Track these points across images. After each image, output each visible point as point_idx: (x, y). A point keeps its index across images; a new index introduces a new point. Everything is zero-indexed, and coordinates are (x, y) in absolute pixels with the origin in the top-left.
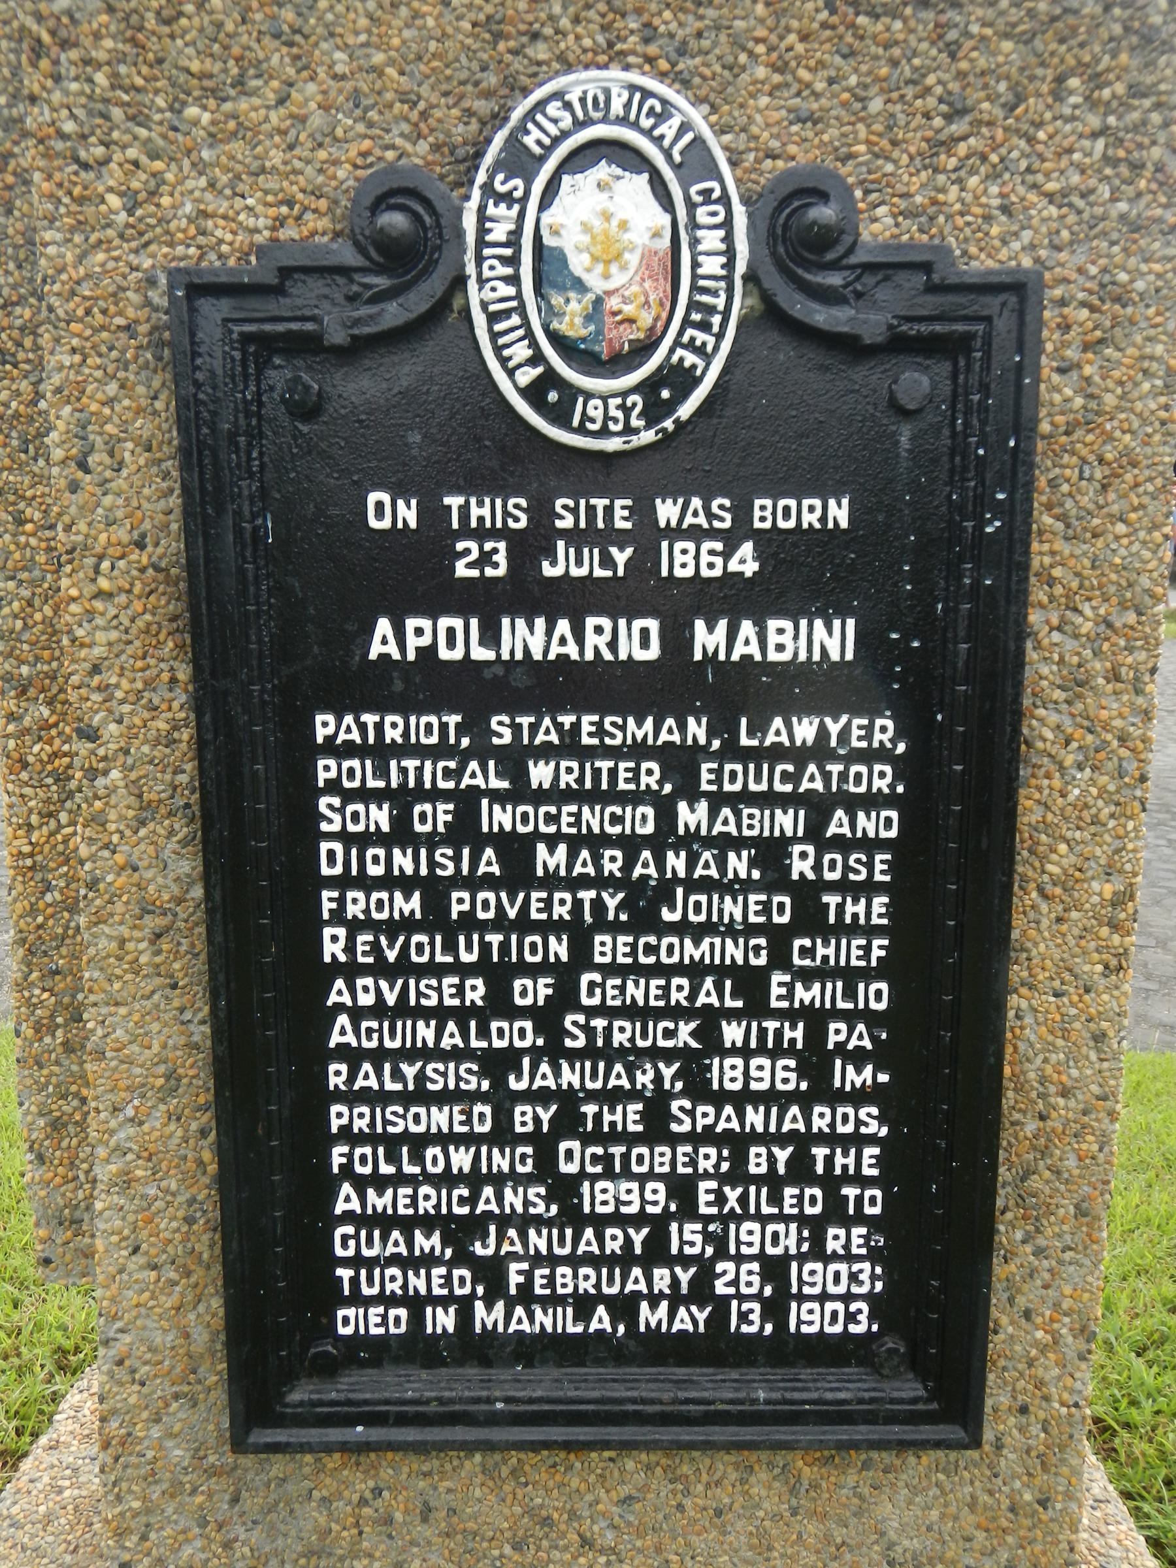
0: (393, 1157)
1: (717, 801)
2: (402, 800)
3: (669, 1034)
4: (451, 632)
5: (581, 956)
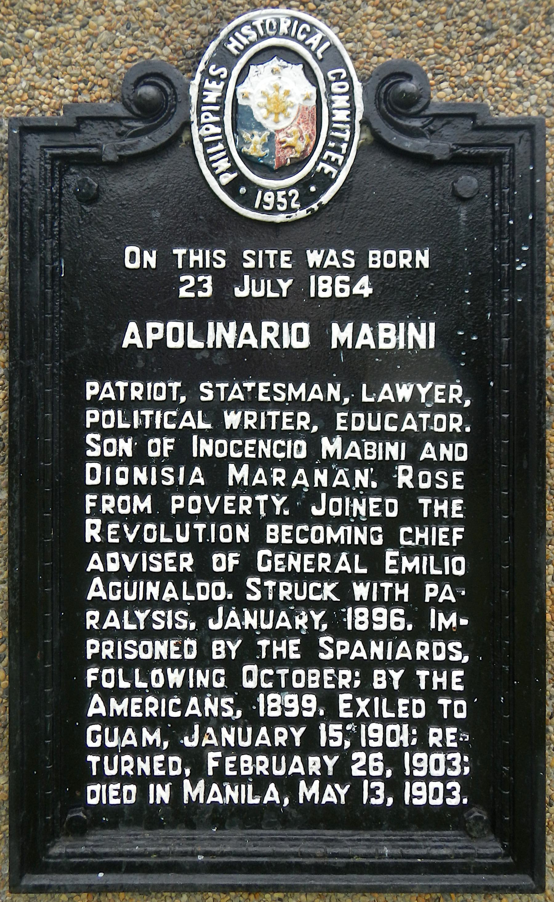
0: (128, 677)
1: (348, 437)
2: (141, 436)
3: (317, 591)
5: (258, 538)
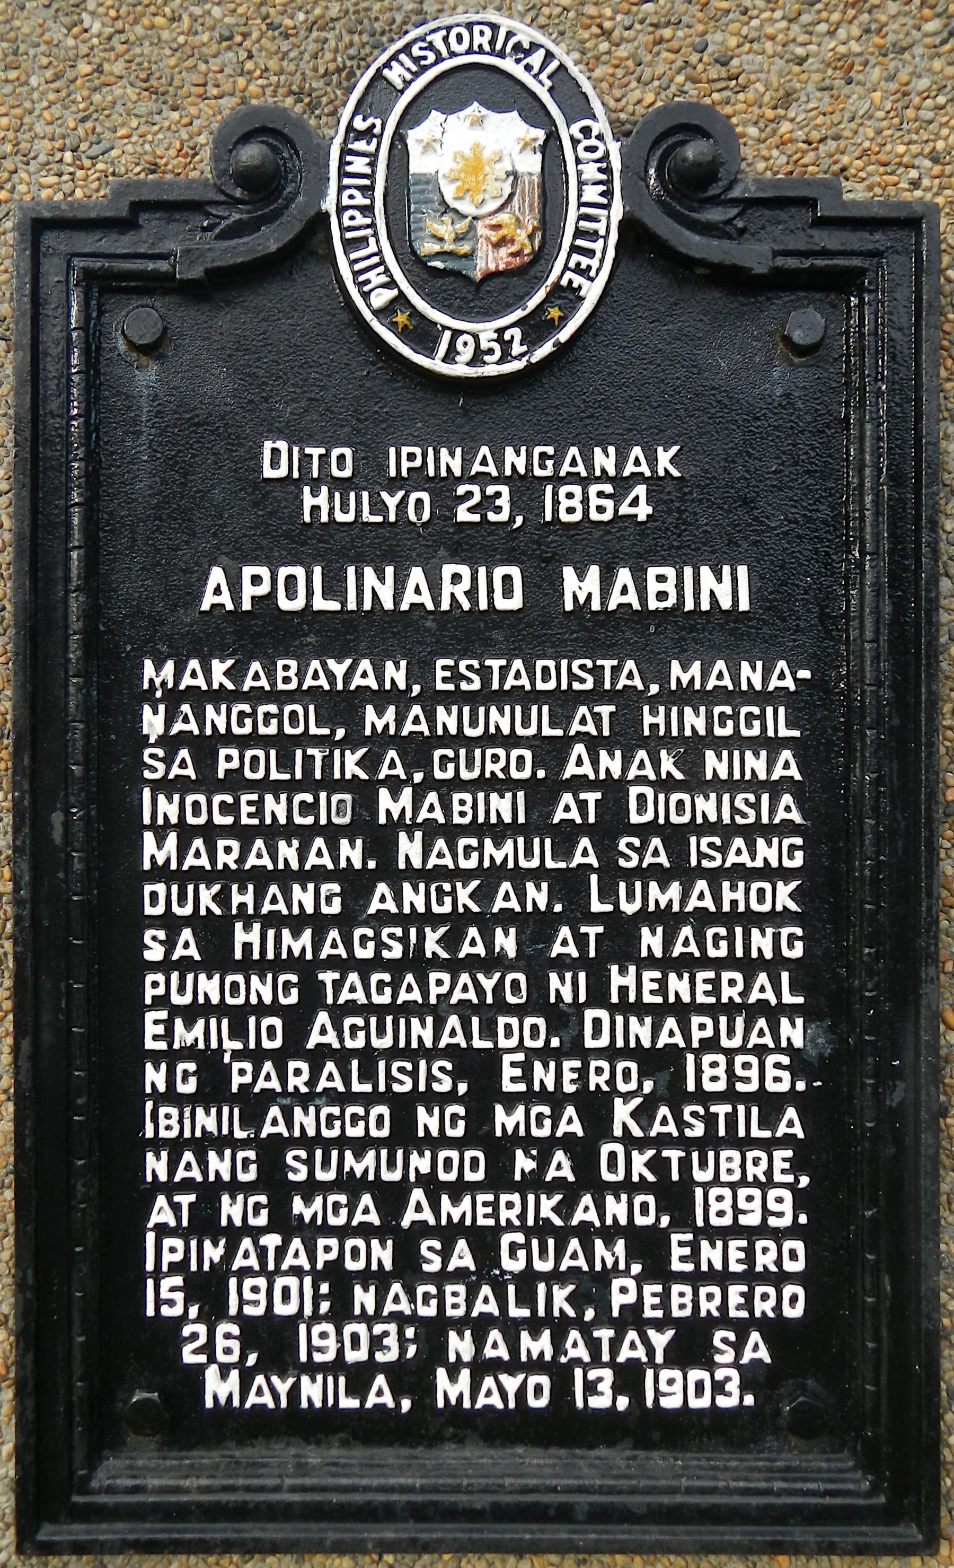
4: (291, 579)
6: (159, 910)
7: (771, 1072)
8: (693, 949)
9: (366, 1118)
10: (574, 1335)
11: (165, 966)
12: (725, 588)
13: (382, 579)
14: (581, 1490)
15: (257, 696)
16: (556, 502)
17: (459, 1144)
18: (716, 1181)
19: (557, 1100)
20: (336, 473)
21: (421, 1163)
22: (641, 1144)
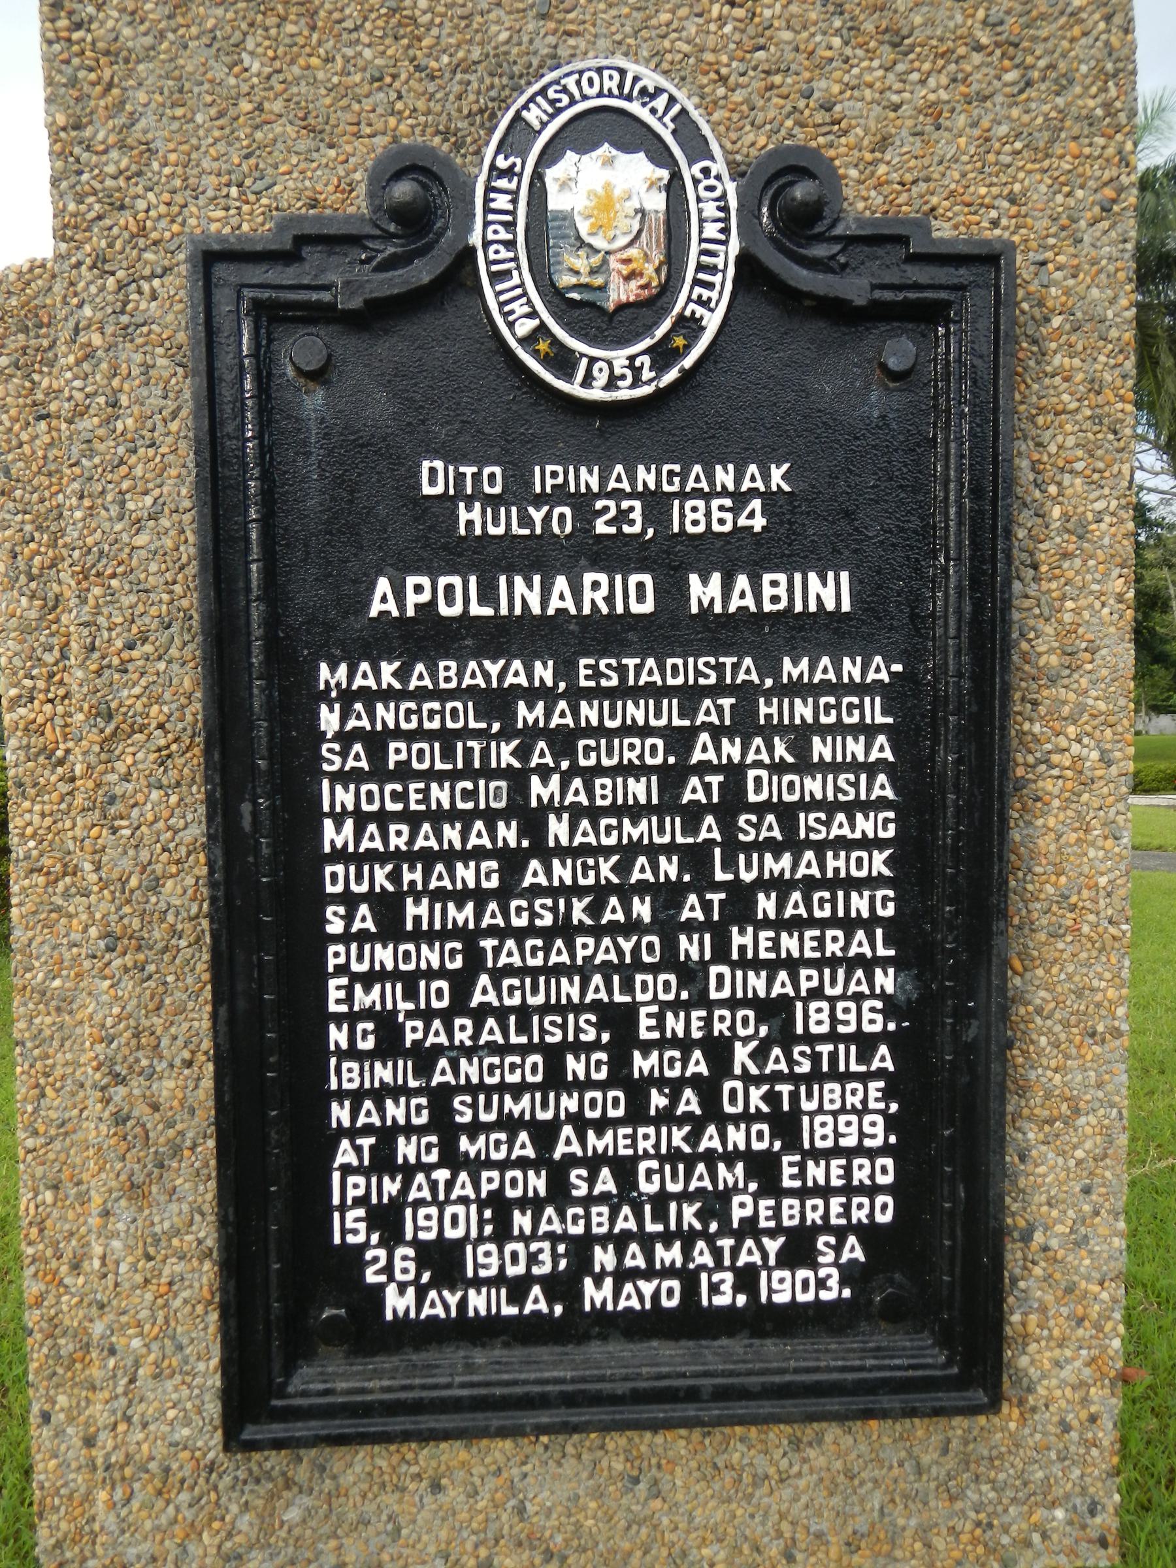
4: (449, 589)
6: (339, 888)
7: (867, 1015)
8: (802, 911)
9: (522, 1066)
10: (701, 1244)
11: (345, 938)
12: (829, 591)
13: (530, 586)
14: (706, 1374)
15: (422, 695)
16: (682, 516)
17: (603, 1086)
18: (820, 1110)
19: (685, 1045)
20: (488, 490)
21: (570, 1103)
22: (758, 1081)
